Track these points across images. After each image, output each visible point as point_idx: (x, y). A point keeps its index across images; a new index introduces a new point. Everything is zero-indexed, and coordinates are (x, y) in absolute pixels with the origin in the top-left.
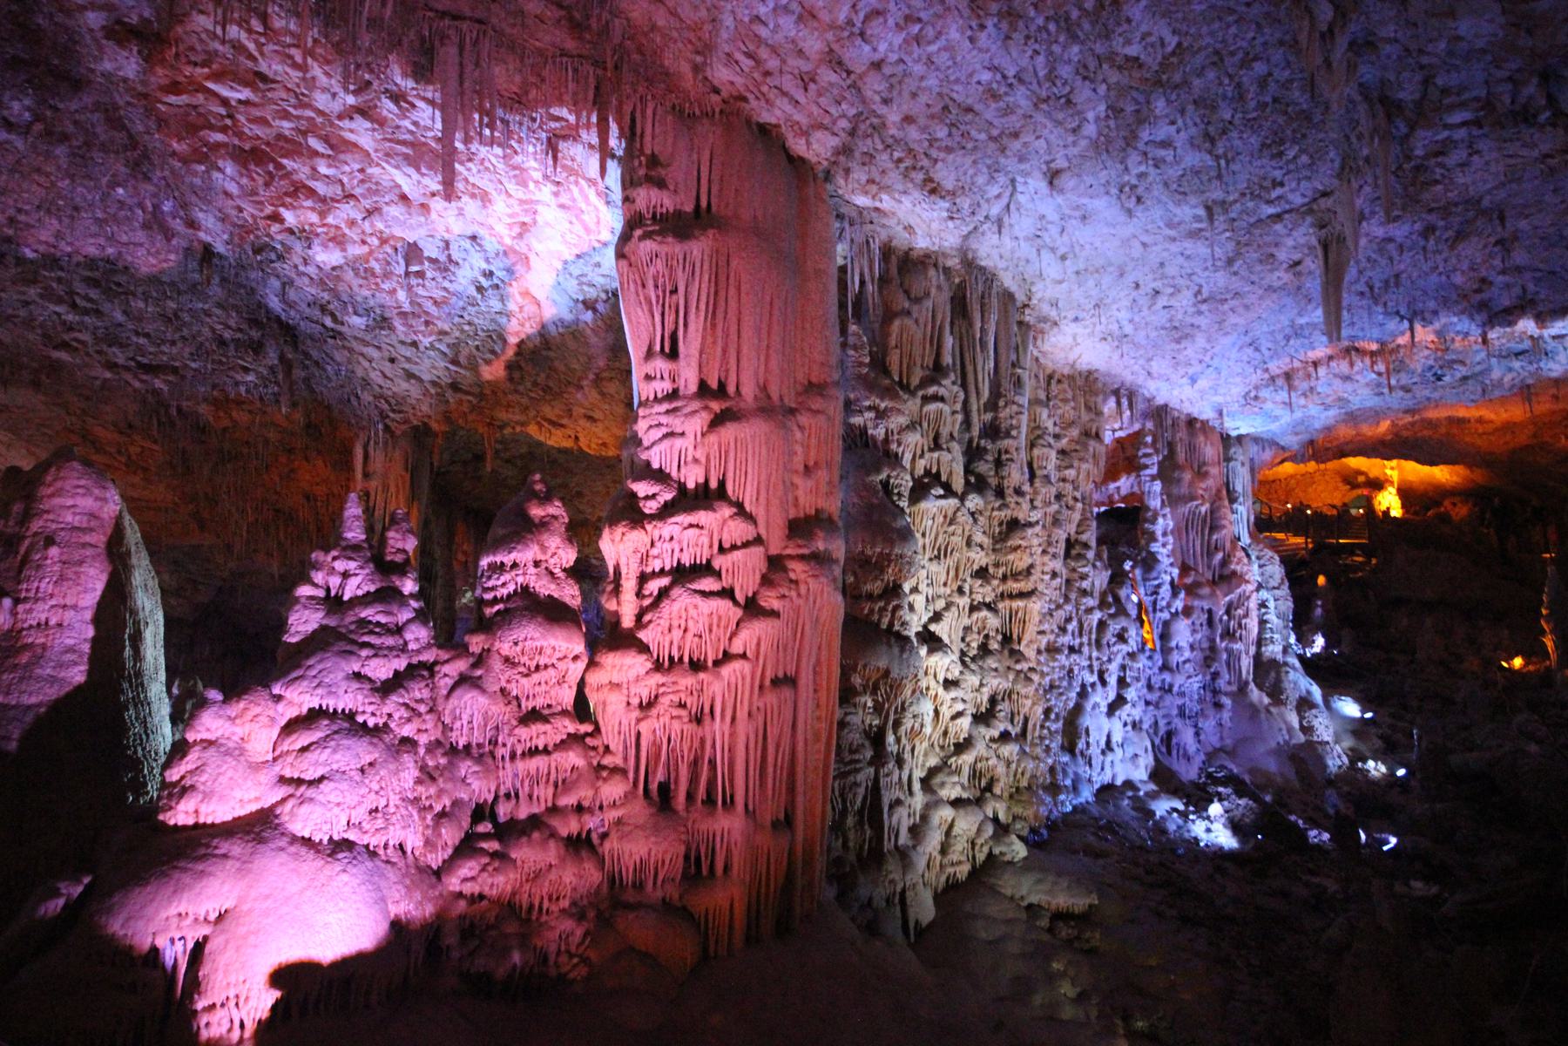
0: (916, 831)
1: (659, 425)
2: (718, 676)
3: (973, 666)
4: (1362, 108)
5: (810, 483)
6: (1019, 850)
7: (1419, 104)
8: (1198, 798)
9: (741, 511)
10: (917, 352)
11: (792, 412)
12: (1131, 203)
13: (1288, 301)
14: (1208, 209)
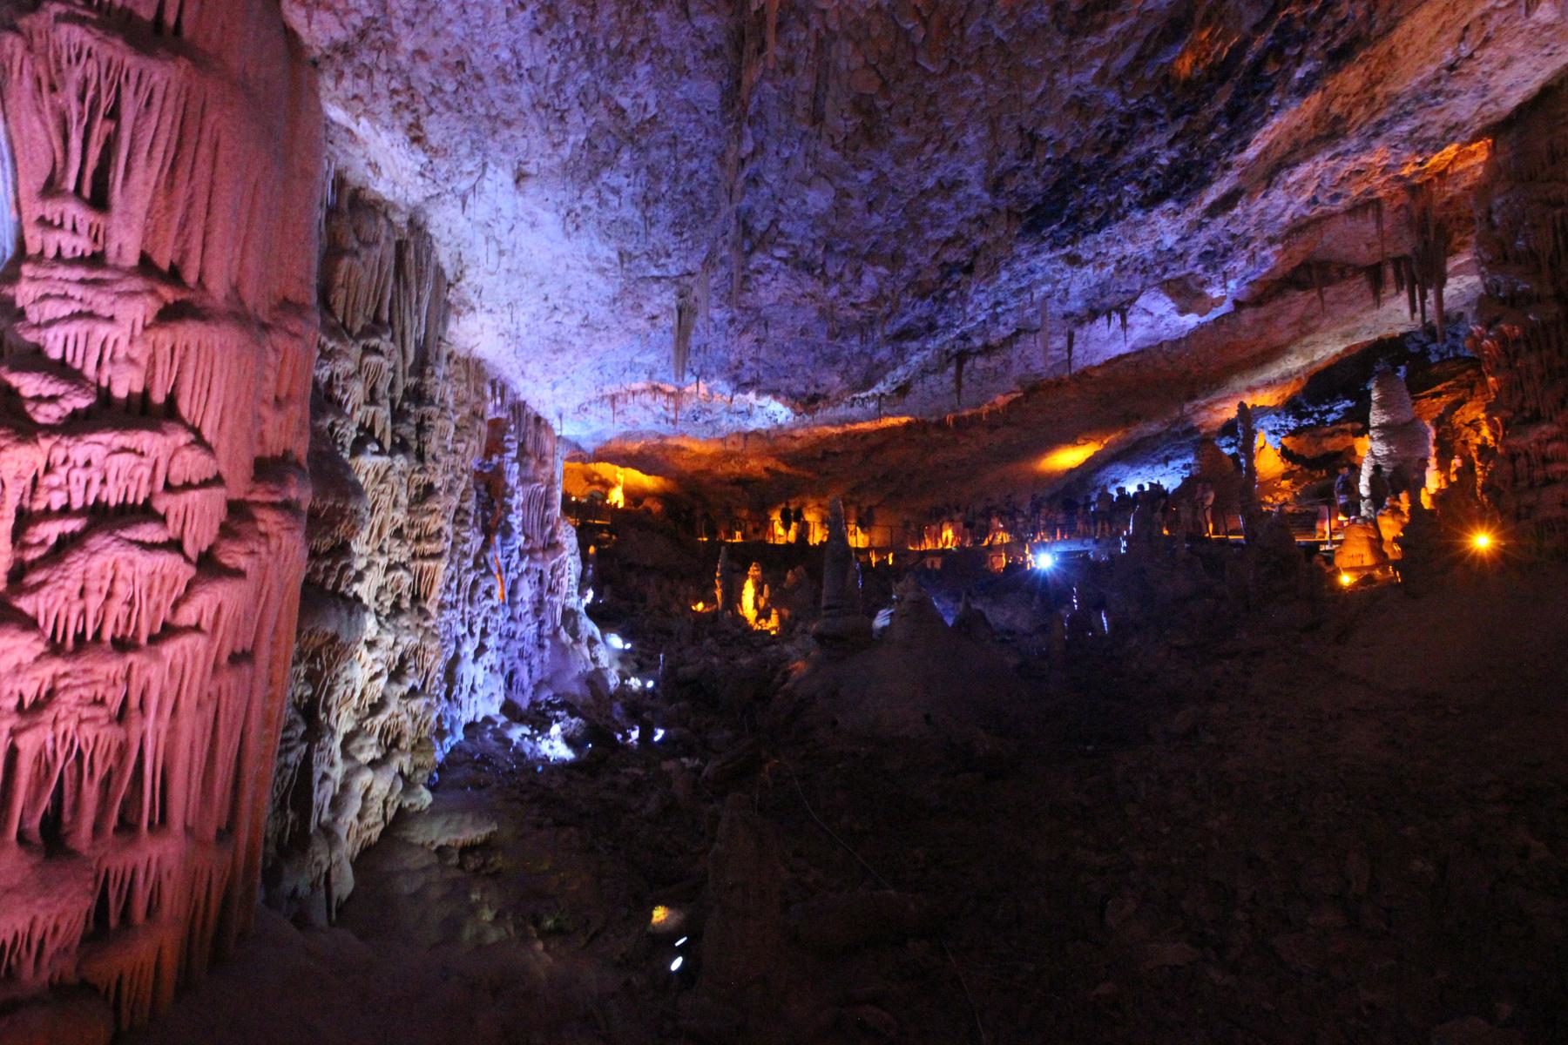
0: (337, 804)
1: (65, 297)
2: (157, 657)
3: (388, 625)
4: (734, 222)
5: (281, 418)
6: (426, 797)
7: (763, 234)
8: (540, 723)
9: (199, 441)
10: (362, 297)
11: (265, 327)
12: (571, 228)
13: (637, 343)
14: (620, 254)
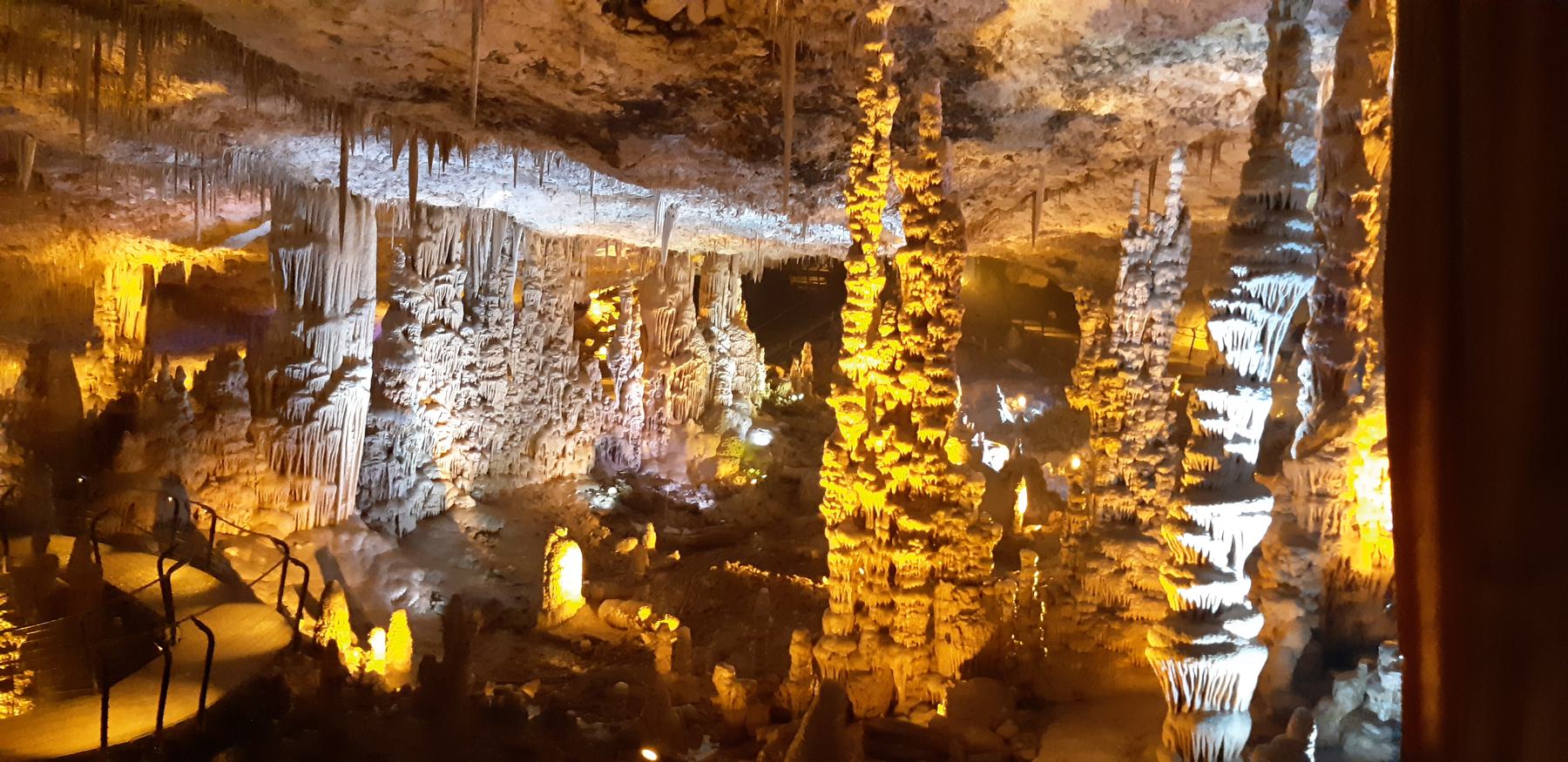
0: (410, 492)
